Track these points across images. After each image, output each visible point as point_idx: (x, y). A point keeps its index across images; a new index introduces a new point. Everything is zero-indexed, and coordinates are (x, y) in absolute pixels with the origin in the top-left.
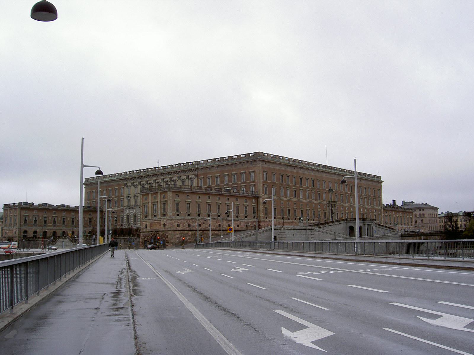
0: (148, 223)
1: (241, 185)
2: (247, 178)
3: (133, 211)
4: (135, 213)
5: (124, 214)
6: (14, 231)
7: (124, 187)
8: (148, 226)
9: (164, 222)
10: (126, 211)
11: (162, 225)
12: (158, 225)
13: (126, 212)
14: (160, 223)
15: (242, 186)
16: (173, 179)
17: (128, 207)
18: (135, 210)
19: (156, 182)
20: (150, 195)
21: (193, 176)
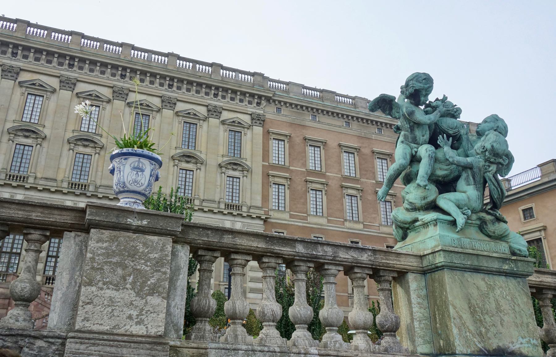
19: (20, 79)
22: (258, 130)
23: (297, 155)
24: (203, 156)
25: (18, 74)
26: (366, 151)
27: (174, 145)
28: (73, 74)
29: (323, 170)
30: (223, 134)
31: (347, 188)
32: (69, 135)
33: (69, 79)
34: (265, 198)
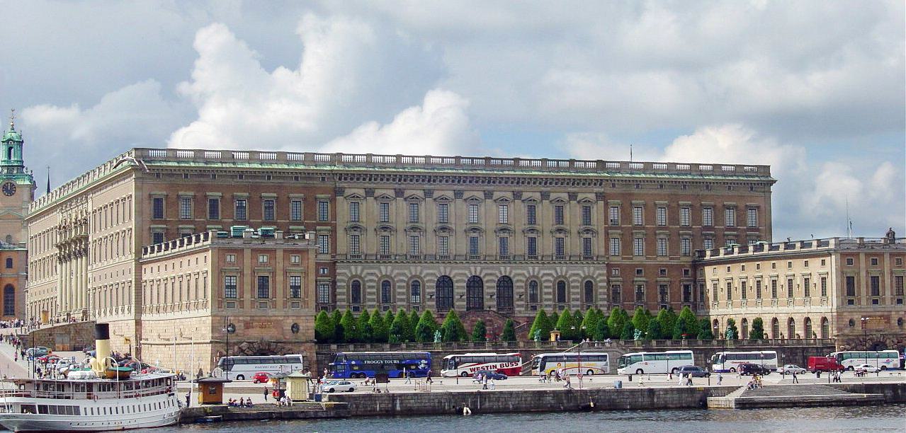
0: (856, 317)
1: (726, 233)
2: (741, 219)
3: (376, 271)
4: (383, 276)
5: (338, 277)
6: (290, 321)
7: (333, 200)
8: (856, 323)
9: (901, 316)
10: (349, 268)
11: (894, 322)
12: (883, 321)
13: (345, 273)
14: (888, 319)
15: (728, 235)
16: (525, 195)
17: (356, 258)
18: (385, 269)
19: (465, 197)
20: (862, 257)
21: (592, 196)
22: (601, 203)
23: (627, 216)
24: (568, 228)
25: (462, 194)
26: (674, 205)
27: (551, 223)
28: (491, 188)
29: (644, 224)
30: (578, 210)
31: (660, 234)
32: (494, 227)
33: (489, 191)
34: (607, 249)
